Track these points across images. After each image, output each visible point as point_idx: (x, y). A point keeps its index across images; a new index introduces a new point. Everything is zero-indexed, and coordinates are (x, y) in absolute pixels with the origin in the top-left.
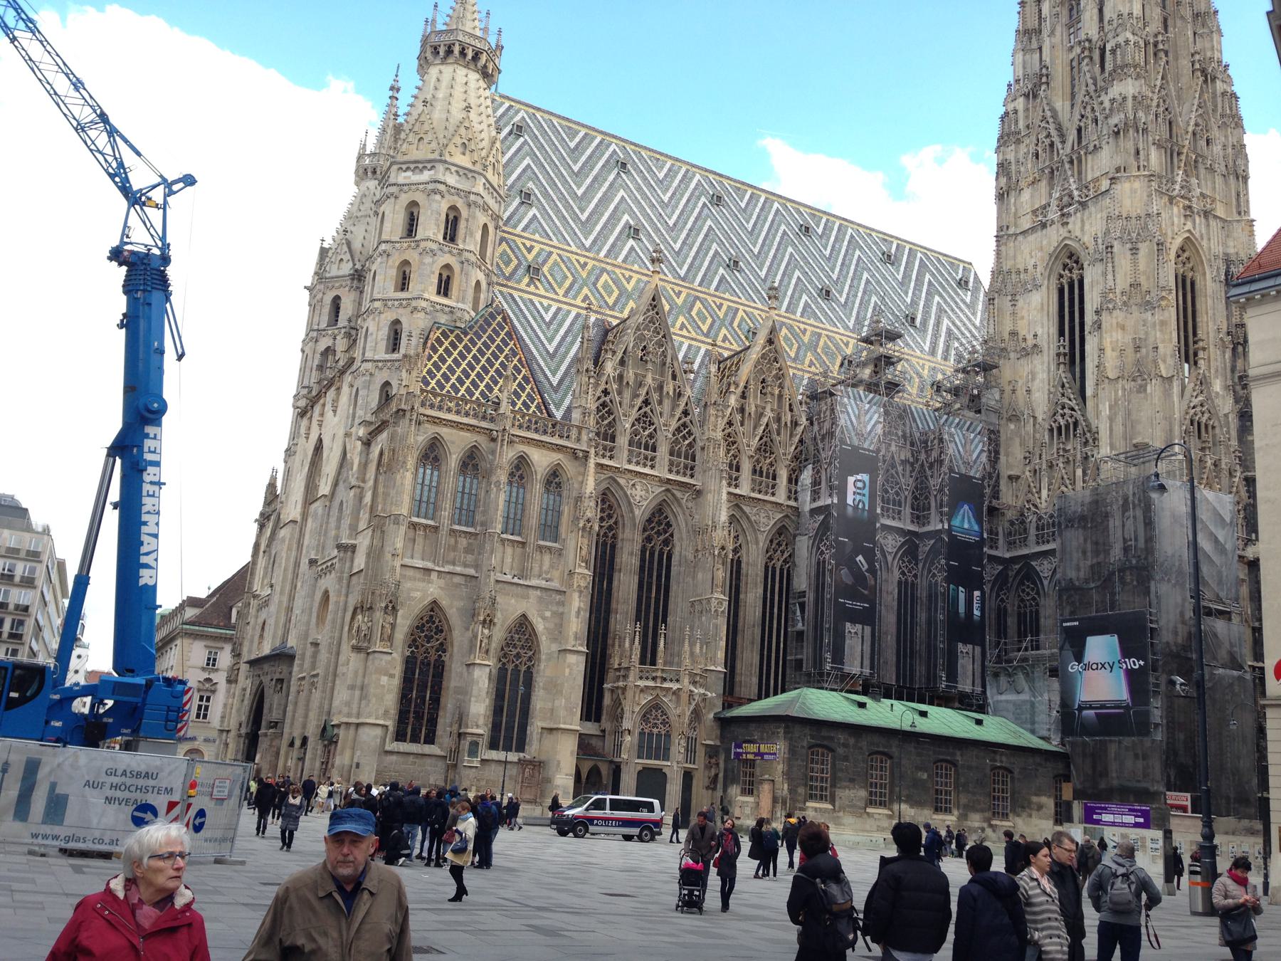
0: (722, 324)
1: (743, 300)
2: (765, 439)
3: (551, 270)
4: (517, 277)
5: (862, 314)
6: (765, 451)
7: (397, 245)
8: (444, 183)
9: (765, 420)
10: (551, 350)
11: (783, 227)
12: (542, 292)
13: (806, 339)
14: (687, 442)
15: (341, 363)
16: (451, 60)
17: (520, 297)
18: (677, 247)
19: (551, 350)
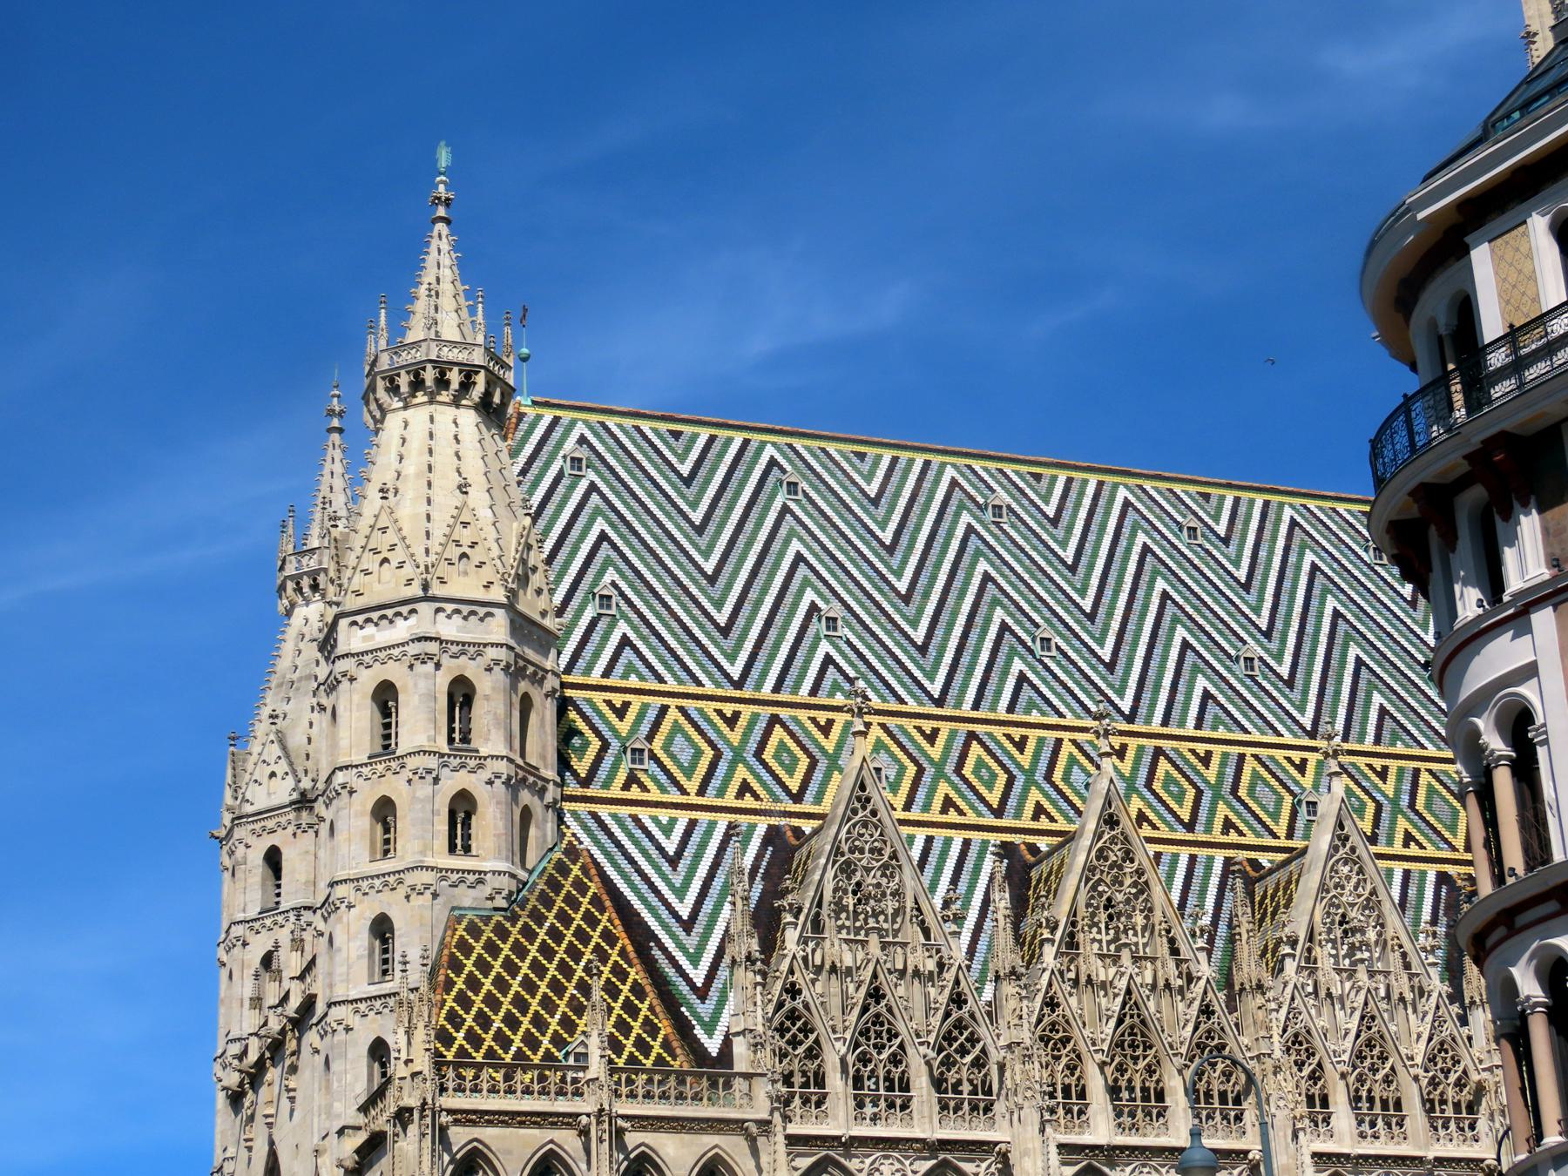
0: (1030, 782)
1: (1070, 720)
2: (1128, 1020)
3: (666, 748)
4: (602, 774)
5: (1330, 690)
6: (1133, 1046)
7: (365, 770)
8: (436, 639)
9: (1122, 984)
10: (685, 913)
11: (1141, 538)
12: (655, 795)
13: (1211, 774)
14: (968, 1059)
15: (295, 1002)
16: (421, 397)
17: (614, 816)
18: (919, 636)
19: (685, 913)
